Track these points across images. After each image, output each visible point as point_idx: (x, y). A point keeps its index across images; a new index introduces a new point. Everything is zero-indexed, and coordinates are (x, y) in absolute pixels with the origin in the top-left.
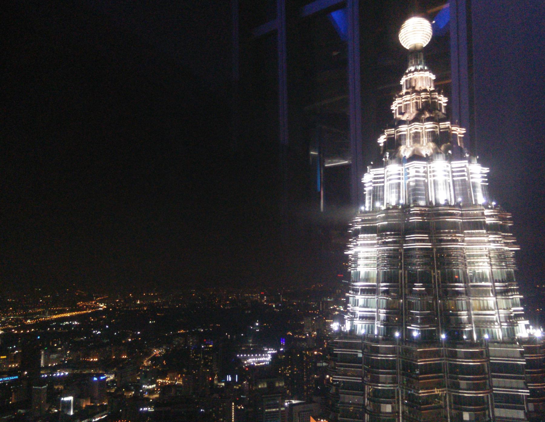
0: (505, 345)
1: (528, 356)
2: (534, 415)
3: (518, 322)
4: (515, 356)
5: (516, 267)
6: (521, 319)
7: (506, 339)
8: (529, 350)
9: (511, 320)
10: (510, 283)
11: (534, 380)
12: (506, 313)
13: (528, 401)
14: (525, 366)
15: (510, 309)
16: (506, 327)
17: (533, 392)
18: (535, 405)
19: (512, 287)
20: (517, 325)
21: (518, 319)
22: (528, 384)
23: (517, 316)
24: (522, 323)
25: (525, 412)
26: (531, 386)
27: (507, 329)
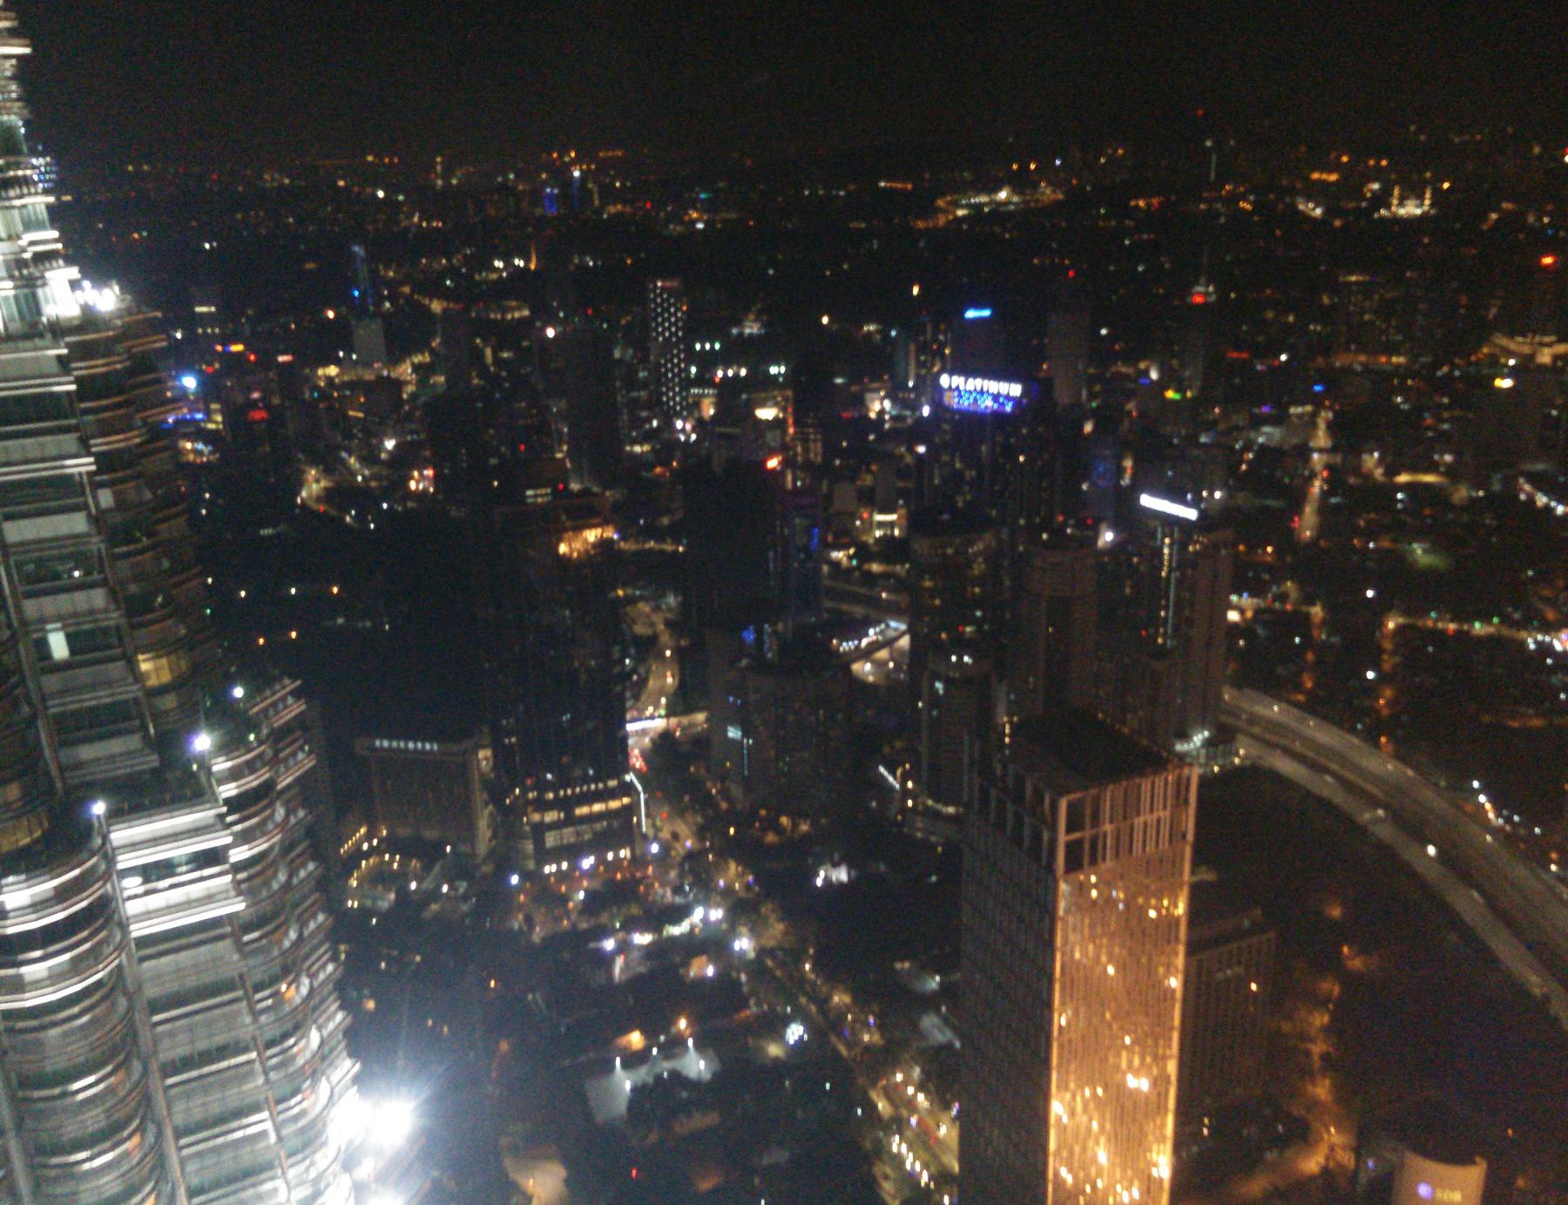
0: (11, 345)
1: (82, 368)
2: (117, 519)
3: (48, 275)
4: (47, 370)
5: (24, 108)
6: (54, 264)
7: (16, 326)
8: (83, 351)
9: (25, 272)
10: (12, 159)
11: (105, 430)
12: (7, 251)
13: (97, 486)
14: (80, 395)
15: (19, 238)
16: (12, 293)
17: (106, 462)
18: (116, 495)
19: (20, 173)
20: (44, 285)
21: (47, 265)
22: (92, 442)
23: (43, 258)
24: (60, 277)
25: (89, 515)
26: (100, 444)
27: (16, 298)
